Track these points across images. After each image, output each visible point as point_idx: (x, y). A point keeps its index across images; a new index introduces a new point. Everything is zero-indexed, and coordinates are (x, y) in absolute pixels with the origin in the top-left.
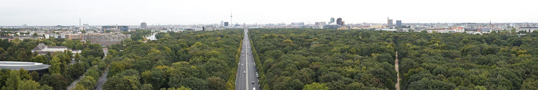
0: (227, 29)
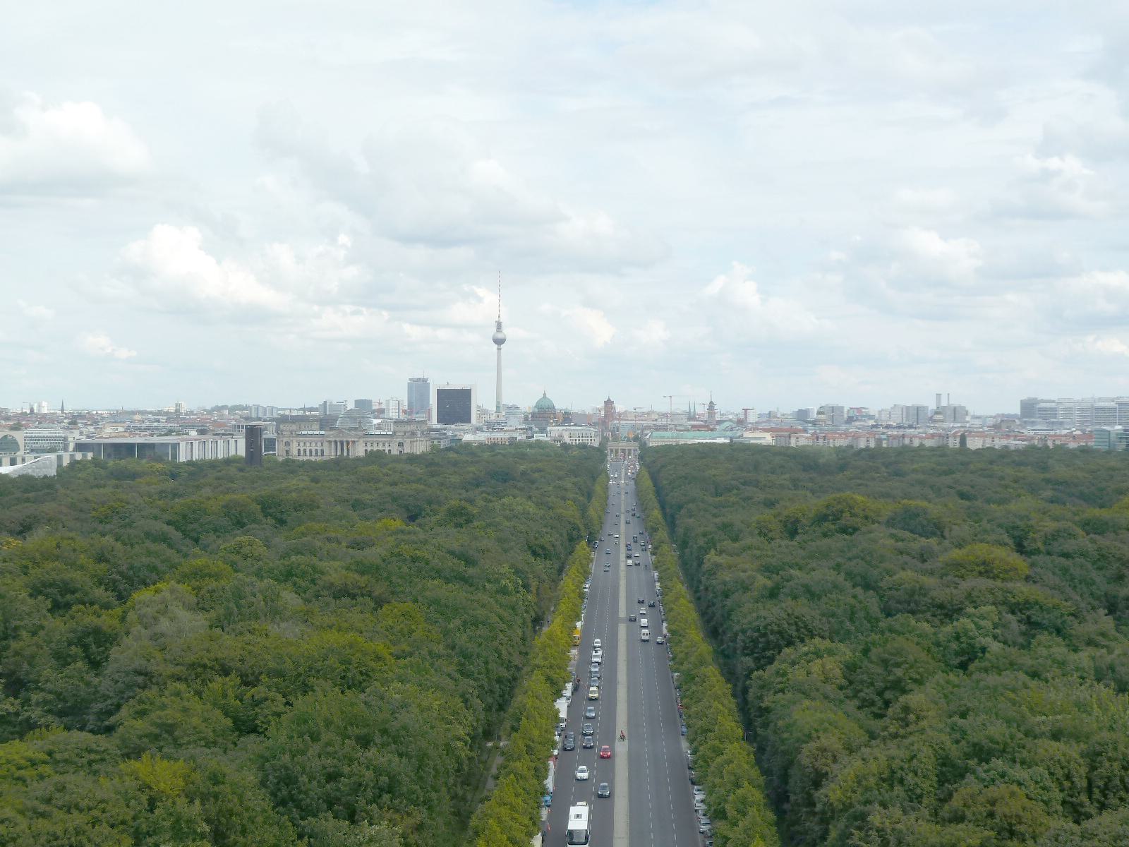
0: (459, 447)
